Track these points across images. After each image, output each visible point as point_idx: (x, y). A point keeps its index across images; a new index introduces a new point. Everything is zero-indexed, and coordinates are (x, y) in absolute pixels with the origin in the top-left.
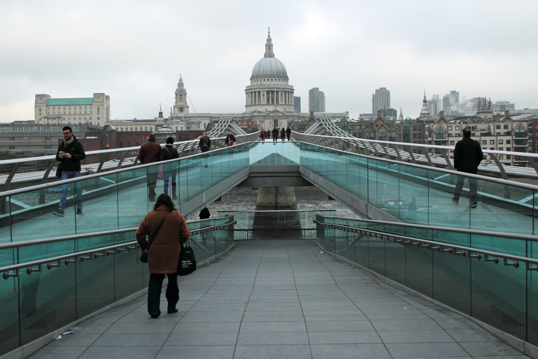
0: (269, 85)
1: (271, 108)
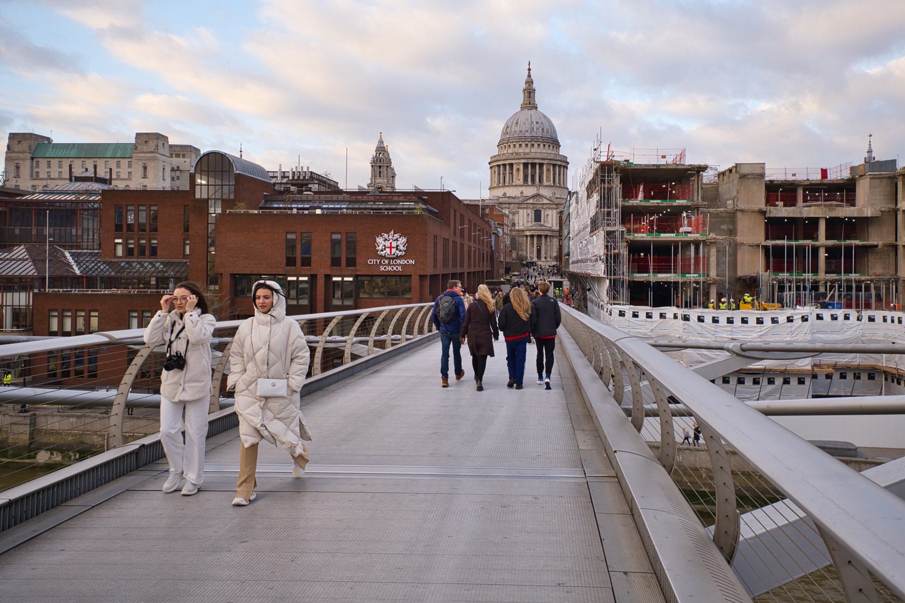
1: (530, 191)
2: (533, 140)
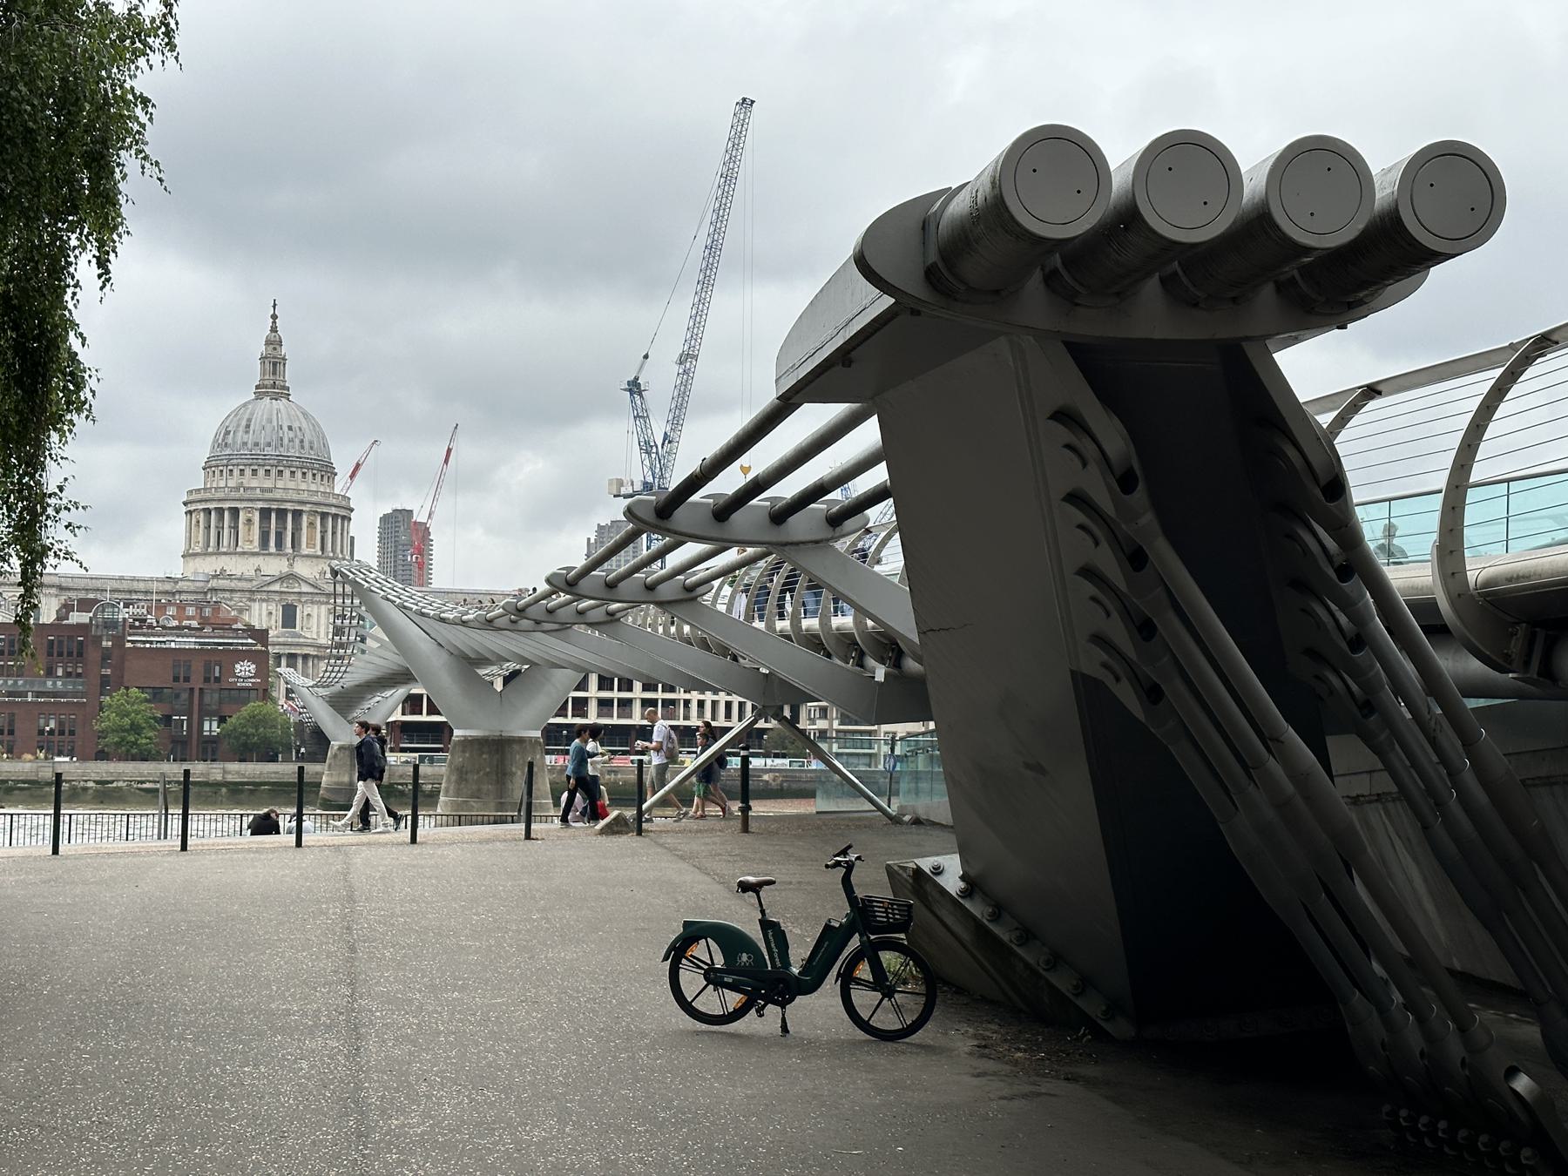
0: (270, 490)
1: (274, 566)
2: (281, 465)
